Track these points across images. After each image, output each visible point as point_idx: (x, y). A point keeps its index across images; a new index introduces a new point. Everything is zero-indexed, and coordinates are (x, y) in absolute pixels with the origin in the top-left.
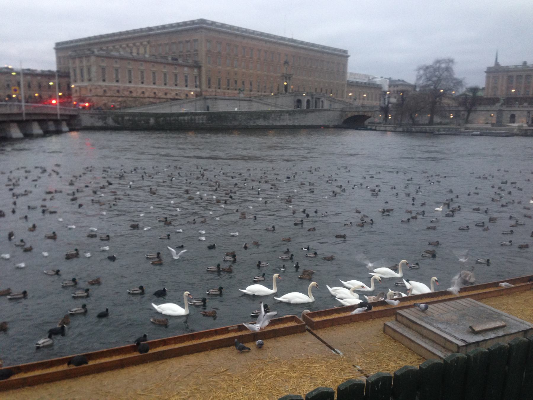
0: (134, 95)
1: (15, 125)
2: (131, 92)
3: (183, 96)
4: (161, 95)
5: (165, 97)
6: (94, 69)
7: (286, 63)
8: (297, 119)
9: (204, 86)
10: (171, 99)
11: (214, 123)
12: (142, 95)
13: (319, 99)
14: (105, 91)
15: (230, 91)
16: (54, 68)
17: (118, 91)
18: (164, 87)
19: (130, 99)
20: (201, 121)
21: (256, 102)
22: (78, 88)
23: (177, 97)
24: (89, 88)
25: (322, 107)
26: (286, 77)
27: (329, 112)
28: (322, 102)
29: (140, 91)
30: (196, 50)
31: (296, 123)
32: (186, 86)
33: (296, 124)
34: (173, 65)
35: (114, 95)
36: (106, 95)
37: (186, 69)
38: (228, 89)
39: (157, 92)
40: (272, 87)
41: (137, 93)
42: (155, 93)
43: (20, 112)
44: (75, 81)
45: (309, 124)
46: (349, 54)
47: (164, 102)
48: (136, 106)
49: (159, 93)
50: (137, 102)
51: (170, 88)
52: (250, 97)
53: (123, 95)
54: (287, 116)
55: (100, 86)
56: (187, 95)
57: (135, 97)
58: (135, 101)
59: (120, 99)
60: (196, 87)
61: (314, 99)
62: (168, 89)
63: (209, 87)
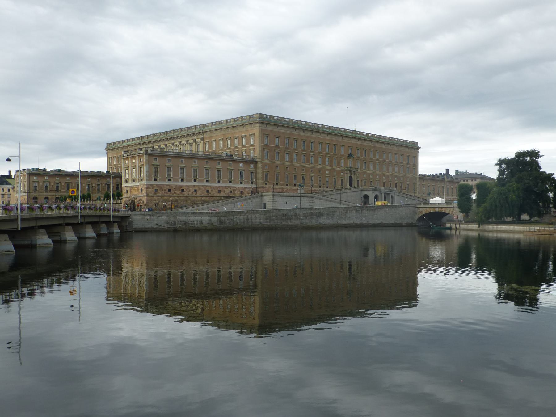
0: (186, 193)
1: (70, 227)
2: (183, 191)
3: (237, 193)
4: (214, 193)
5: (218, 195)
7: (350, 155)
8: (366, 216)
9: (260, 182)
10: (224, 197)
11: (272, 222)
12: (194, 194)
13: (388, 194)
14: (156, 191)
15: (288, 187)
16: (104, 170)
17: (170, 191)
18: (218, 185)
19: (182, 198)
20: (258, 221)
21: (317, 198)
22: (128, 189)
23: (231, 195)
24: (140, 188)
25: (392, 203)
26: (350, 171)
27: (401, 209)
28: (392, 197)
29: (192, 190)
30: (253, 146)
31: (364, 221)
32: (241, 183)
33: (365, 222)
34: (227, 161)
35: (166, 194)
36: (158, 195)
37: (241, 165)
38: (287, 185)
40: (335, 182)
41: (189, 191)
42: (208, 191)
43: (76, 214)
44: (127, 182)
45: (379, 222)
46: (419, 145)
47: (218, 200)
48: (188, 205)
49: (212, 191)
50: (189, 201)
51: (224, 185)
52: (312, 193)
53: (175, 194)
54: (354, 213)
55: (152, 185)
56: (242, 192)
57: (186, 196)
58: (187, 200)
59: (171, 199)
60: (252, 183)
61: (383, 195)
62: (222, 187)
63: (266, 184)
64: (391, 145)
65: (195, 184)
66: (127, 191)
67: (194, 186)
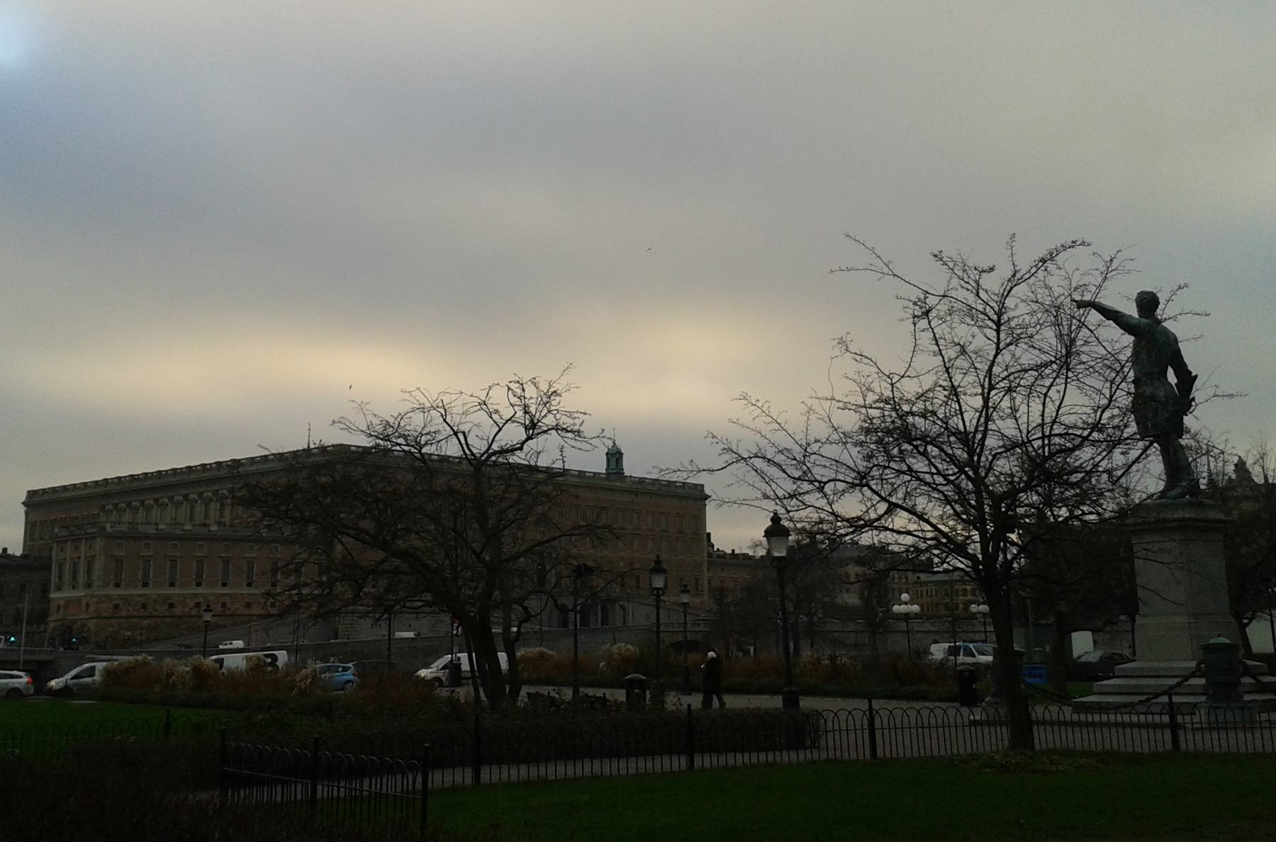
0: (178, 611)
2: (172, 606)
5: (246, 612)
6: (98, 564)
10: (260, 616)
12: (194, 612)
14: (116, 607)
17: (144, 606)
18: (246, 591)
19: (168, 620)
22: (61, 602)
28: (622, 607)
29: (191, 603)
35: (135, 614)
39: (228, 602)
42: (224, 605)
44: (59, 589)
46: (707, 491)
55: (107, 596)
59: (146, 622)
64: (636, 493)
65: (200, 590)
66: (59, 608)
67: (196, 595)
